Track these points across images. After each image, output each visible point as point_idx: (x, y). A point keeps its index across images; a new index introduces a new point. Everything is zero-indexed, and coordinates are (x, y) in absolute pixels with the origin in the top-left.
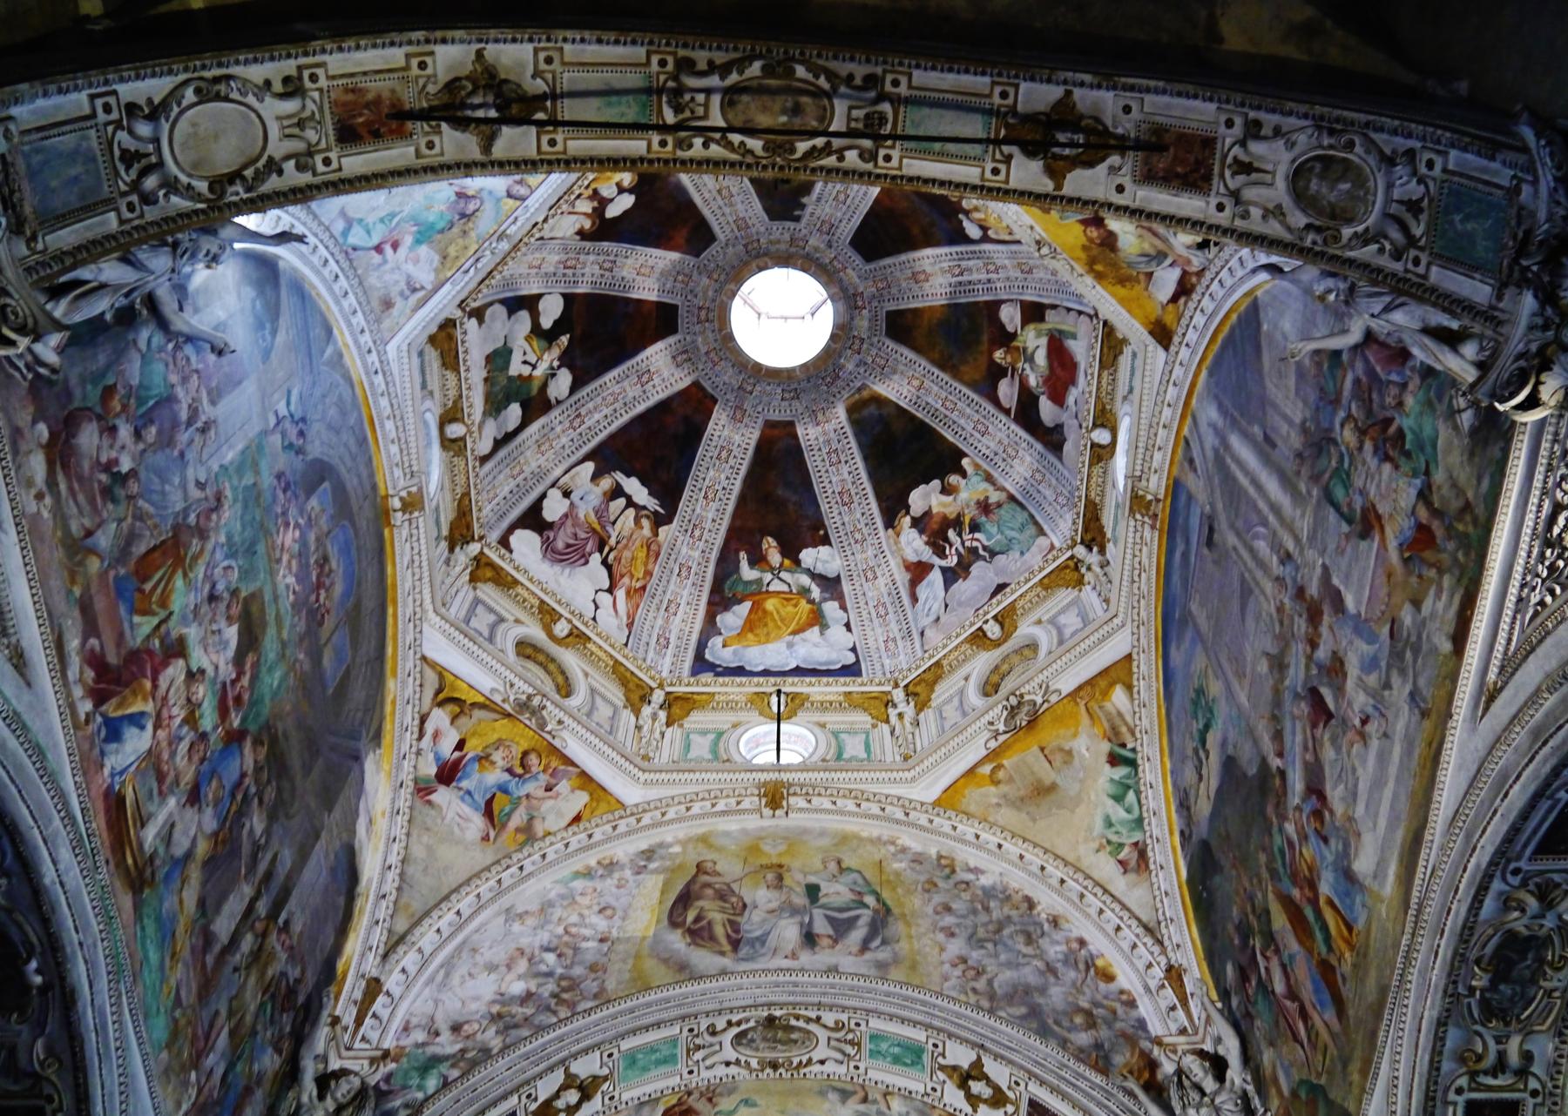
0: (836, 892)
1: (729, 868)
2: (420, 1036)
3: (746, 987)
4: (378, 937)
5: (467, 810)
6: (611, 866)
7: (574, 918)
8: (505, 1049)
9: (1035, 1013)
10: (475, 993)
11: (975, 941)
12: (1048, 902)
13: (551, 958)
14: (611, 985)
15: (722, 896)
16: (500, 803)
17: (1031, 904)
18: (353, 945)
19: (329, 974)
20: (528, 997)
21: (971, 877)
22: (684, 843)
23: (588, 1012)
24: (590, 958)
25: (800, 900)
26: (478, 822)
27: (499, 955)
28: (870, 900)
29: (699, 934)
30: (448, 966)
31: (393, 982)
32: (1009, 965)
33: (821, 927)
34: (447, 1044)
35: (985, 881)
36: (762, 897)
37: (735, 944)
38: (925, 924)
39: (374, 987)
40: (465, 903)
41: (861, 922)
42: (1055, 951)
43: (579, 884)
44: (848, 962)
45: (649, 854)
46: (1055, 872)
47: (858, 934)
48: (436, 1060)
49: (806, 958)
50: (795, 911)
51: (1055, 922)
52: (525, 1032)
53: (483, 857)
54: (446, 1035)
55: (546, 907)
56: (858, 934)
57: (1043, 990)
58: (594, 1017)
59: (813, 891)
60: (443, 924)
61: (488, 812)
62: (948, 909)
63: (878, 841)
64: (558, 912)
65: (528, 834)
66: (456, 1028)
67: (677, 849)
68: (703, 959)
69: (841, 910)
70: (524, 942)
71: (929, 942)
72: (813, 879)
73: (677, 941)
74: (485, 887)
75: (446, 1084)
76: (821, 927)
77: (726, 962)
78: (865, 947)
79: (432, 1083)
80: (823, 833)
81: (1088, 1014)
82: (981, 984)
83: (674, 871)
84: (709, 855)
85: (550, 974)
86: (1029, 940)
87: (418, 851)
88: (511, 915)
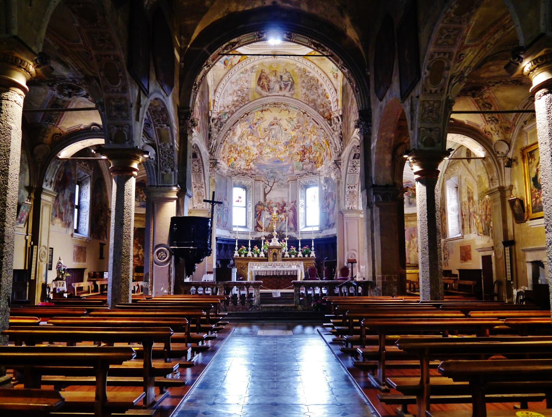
0: (285, 78)
1: (267, 71)
2: (222, 108)
3: (271, 100)
4: (213, 92)
5: (221, 64)
6: (246, 71)
7: (242, 84)
8: (236, 111)
9: (315, 105)
10: (229, 100)
11: (308, 90)
12: (321, 81)
13: (239, 92)
14: (250, 98)
15: (266, 79)
16: (227, 62)
17: (318, 81)
18: (210, 97)
19: (209, 103)
20: (237, 101)
21: (308, 74)
22: (259, 65)
23: (247, 104)
24: (246, 92)
25: (279, 79)
26: (223, 65)
27: (230, 91)
28: (291, 79)
29: (263, 87)
30: (224, 94)
31: (216, 99)
32: (313, 95)
33: (283, 86)
34: (227, 110)
35: (311, 75)
36: (272, 78)
37: (269, 89)
38: (300, 85)
39: (214, 101)
40: (224, 82)
41: (289, 85)
42: (320, 92)
43: (242, 75)
44: (287, 94)
45: (253, 68)
46: (323, 75)
47: (289, 87)
48: (226, 113)
49: (281, 93)
50: (279, 82)
51: (321, 85)
52: (238, 108)
53: (226, 71)
54: (226, 108)
55: (237, 80)
56: (289, 87)
57: (317, 100)
58: (248, 105)
59: (281, 77)
60: (221, 87)
61: (225, 63)
62: (304, 82)
63: (293, 65)
64: (239, 82)
65: (231, 64)
66: (228, 107)
67: (257, 66)
68: (264, 93)
69: (286, 82)
70: (235, 88)
71: (300, 90)
72: (281, 74)
73: (259, 88)
74: (226, 78)
75: (228, 118)
76: (283, 86)
77: (267, 93)
78: (290, 91)
79: (227, 117)
80: (283, 62)
81: (323, 105)
82: (307, 99)
83: (257, 72)
84: (264, 68)
85: (240, 96)
86: (316, 89)
87: (215, 74)
88: (232, 83)
